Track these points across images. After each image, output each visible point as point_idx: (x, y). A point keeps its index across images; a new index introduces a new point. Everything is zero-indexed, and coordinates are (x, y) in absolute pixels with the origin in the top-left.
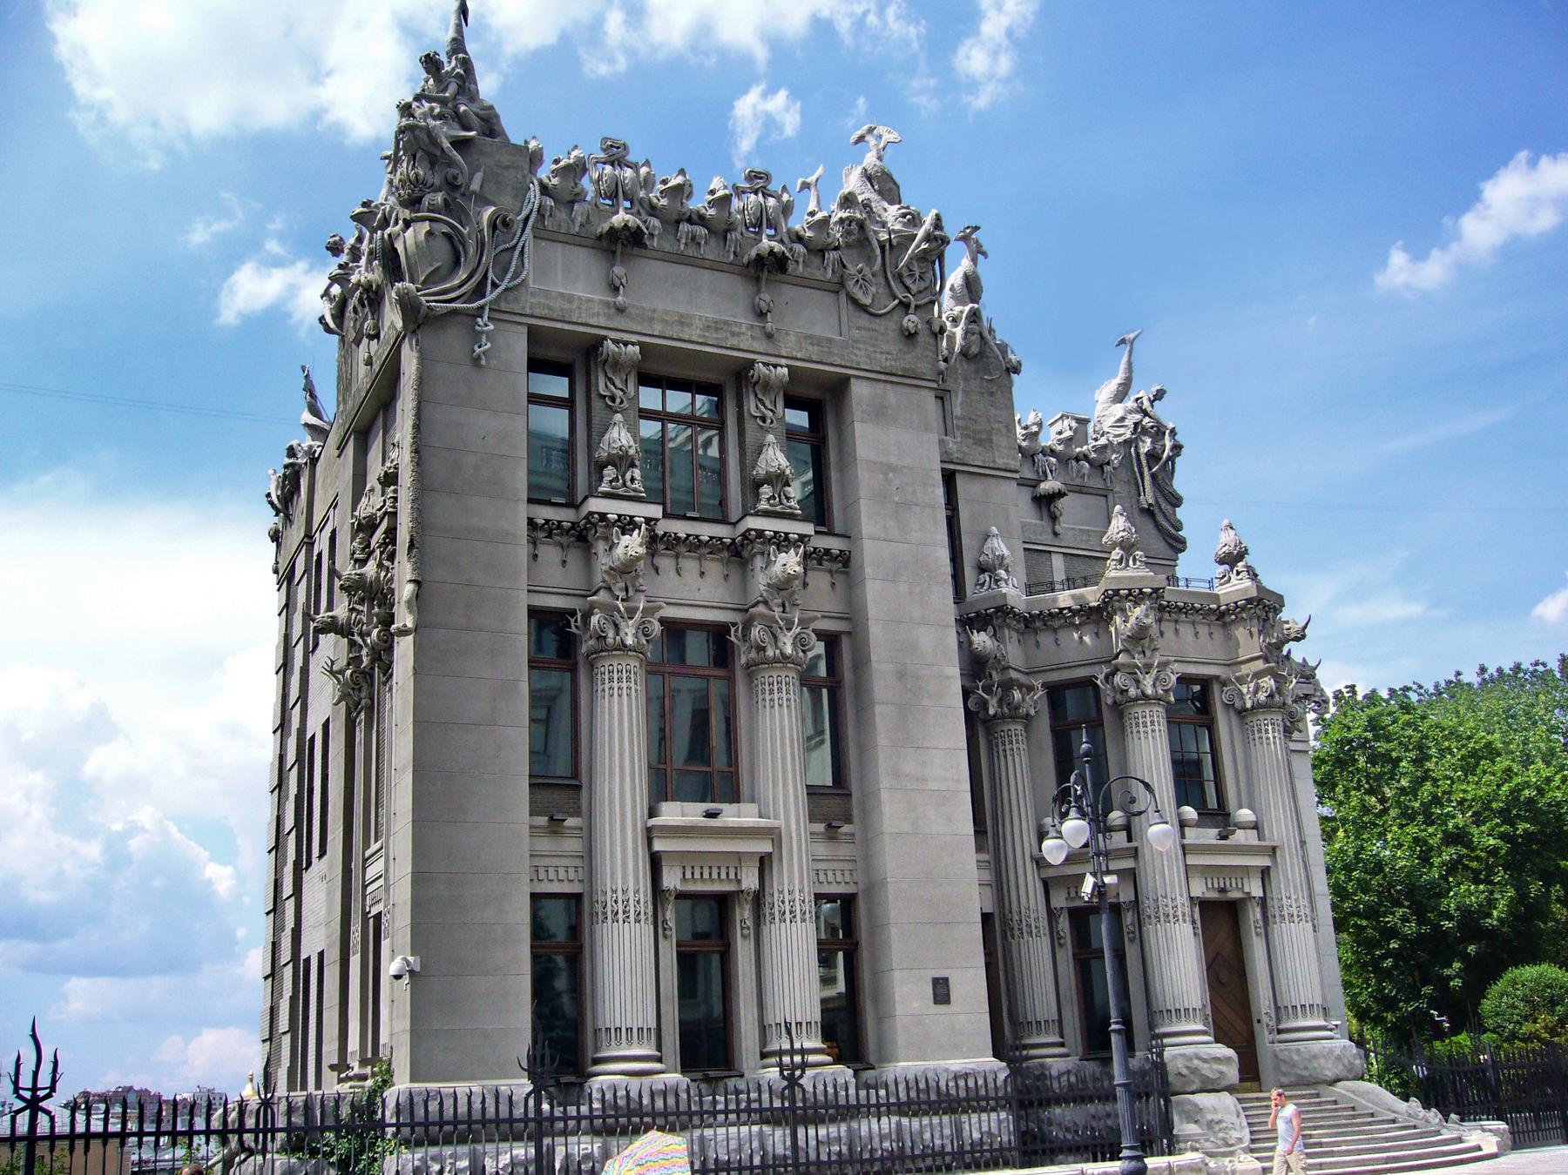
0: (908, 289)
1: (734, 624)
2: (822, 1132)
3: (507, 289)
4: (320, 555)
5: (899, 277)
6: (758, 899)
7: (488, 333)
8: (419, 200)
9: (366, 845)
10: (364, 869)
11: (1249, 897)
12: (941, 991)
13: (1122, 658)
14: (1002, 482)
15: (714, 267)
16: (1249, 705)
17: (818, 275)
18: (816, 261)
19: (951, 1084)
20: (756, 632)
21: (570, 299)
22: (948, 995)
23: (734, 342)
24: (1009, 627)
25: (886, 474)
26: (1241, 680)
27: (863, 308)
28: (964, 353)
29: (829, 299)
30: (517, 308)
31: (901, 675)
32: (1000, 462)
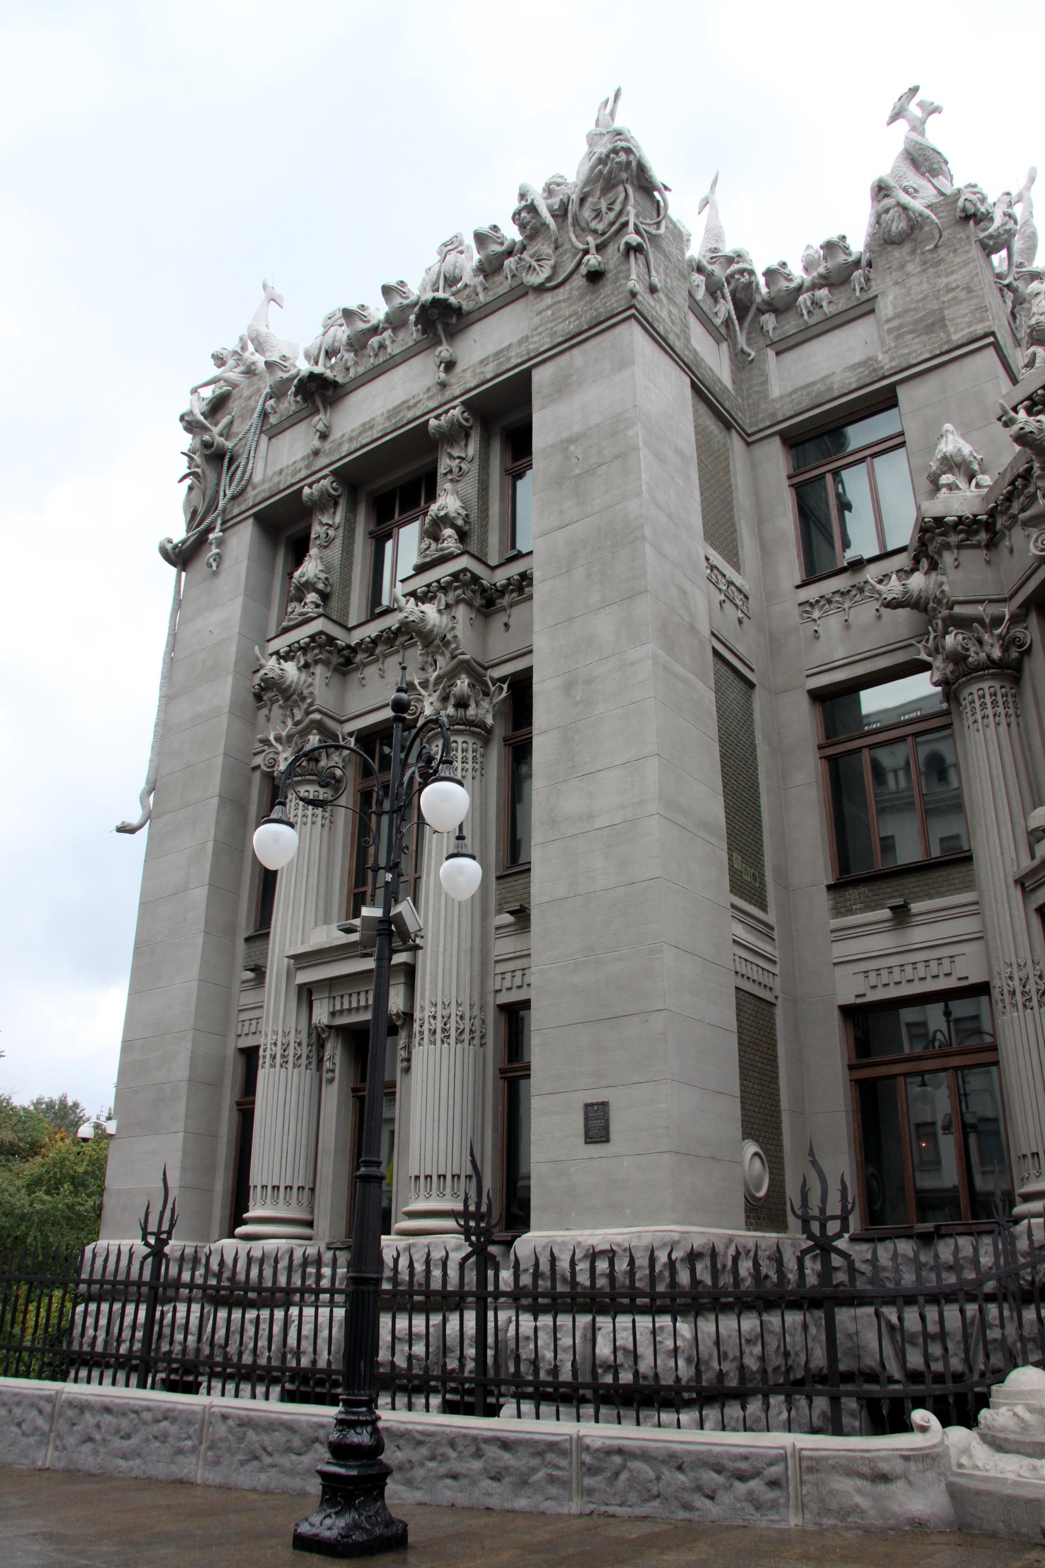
2: (402, 1323)
3: (234, 498)
7: (220, 542)
12: (597, 1126)
14: (968, 362)
15: (407, 355)
17: (502, 290)
18: (498, 279)
19: (583, 1266)
21: (281, 472)
22: (606, 1128)
23: (410, 415)
24: (947, 546)
25: (566, 449)
27: (541, 289)
28: (885, 240)
29: (518, 307)
30: (243, 507)
31: (568, 687)
32: (957, 337)
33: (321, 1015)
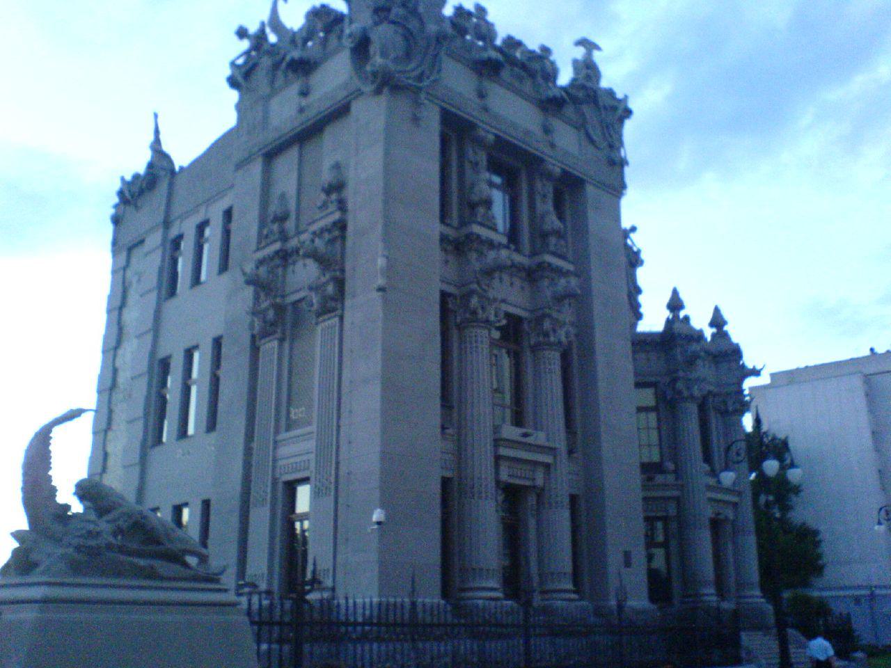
0: (611, 136)
1: (526, 319)
3: (435, 81)
4: (180, 237)
5: (607, 127)
6: (540, 493)
9: (277, 432)
10: (275, 448)
11: (727, 519)
13: (681, 373)
15: (526, 97)
16: (730, 409)
20: (547, 325)
26: (728, 394)
27: (592, 141)
29: (574, 130)
33: (504, 476)
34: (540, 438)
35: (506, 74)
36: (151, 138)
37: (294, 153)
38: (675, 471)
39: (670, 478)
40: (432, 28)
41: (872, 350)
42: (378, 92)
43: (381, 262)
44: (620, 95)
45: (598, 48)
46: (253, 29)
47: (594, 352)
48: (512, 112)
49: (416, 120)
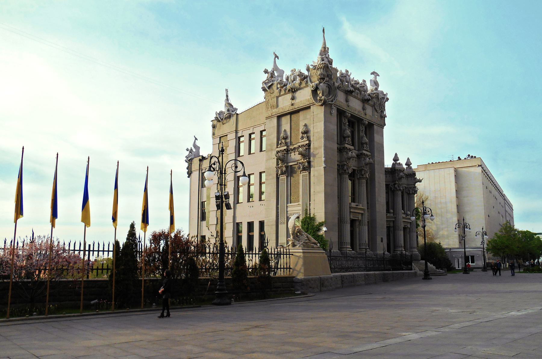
8: (324, 79)
9: (287, 203)
12: (382, 241)
20: (363, 172)
26: (411, 188)
27: (376, 111)
33: (352, 217)
34: (360, 206)
35: (353, 94)
36: (225, 98)
37: (289, 117)
38: (393, 213)
39: (392, 215)
40: (337, 84)
41: (459, 158)
42: (322, 105)
43: (323, 159)
44: (385, 93)
45: (379, 76)
46: (270, 70)
47: (375, 179)
48: (355, 106)
49: (331, 114)
